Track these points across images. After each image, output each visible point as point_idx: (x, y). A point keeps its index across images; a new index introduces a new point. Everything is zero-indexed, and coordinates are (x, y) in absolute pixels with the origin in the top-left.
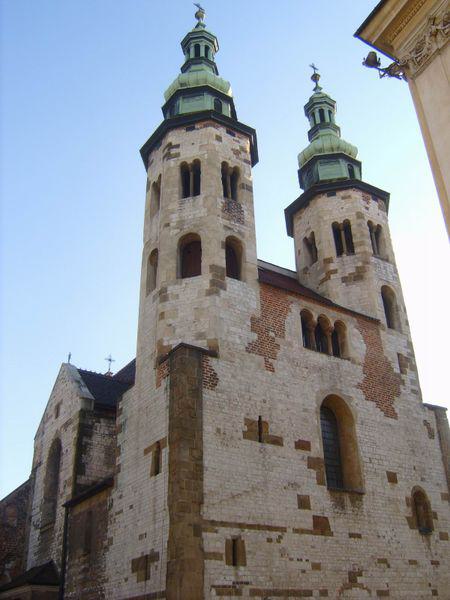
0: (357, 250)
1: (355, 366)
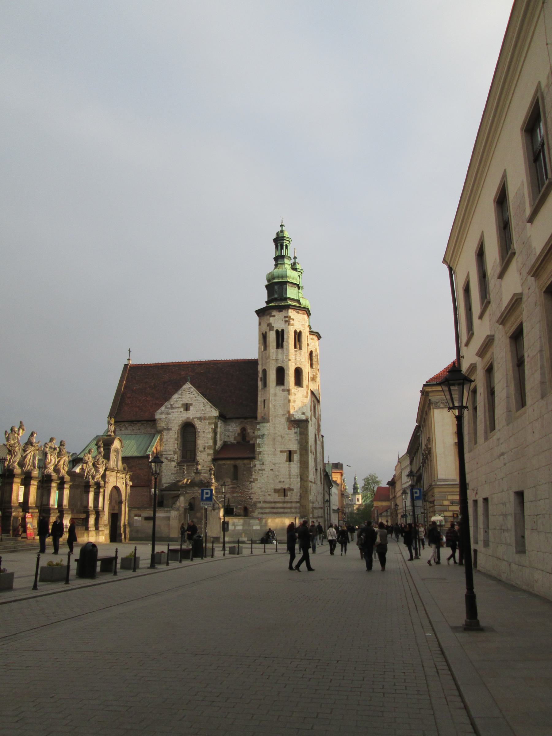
0: (314, 367)
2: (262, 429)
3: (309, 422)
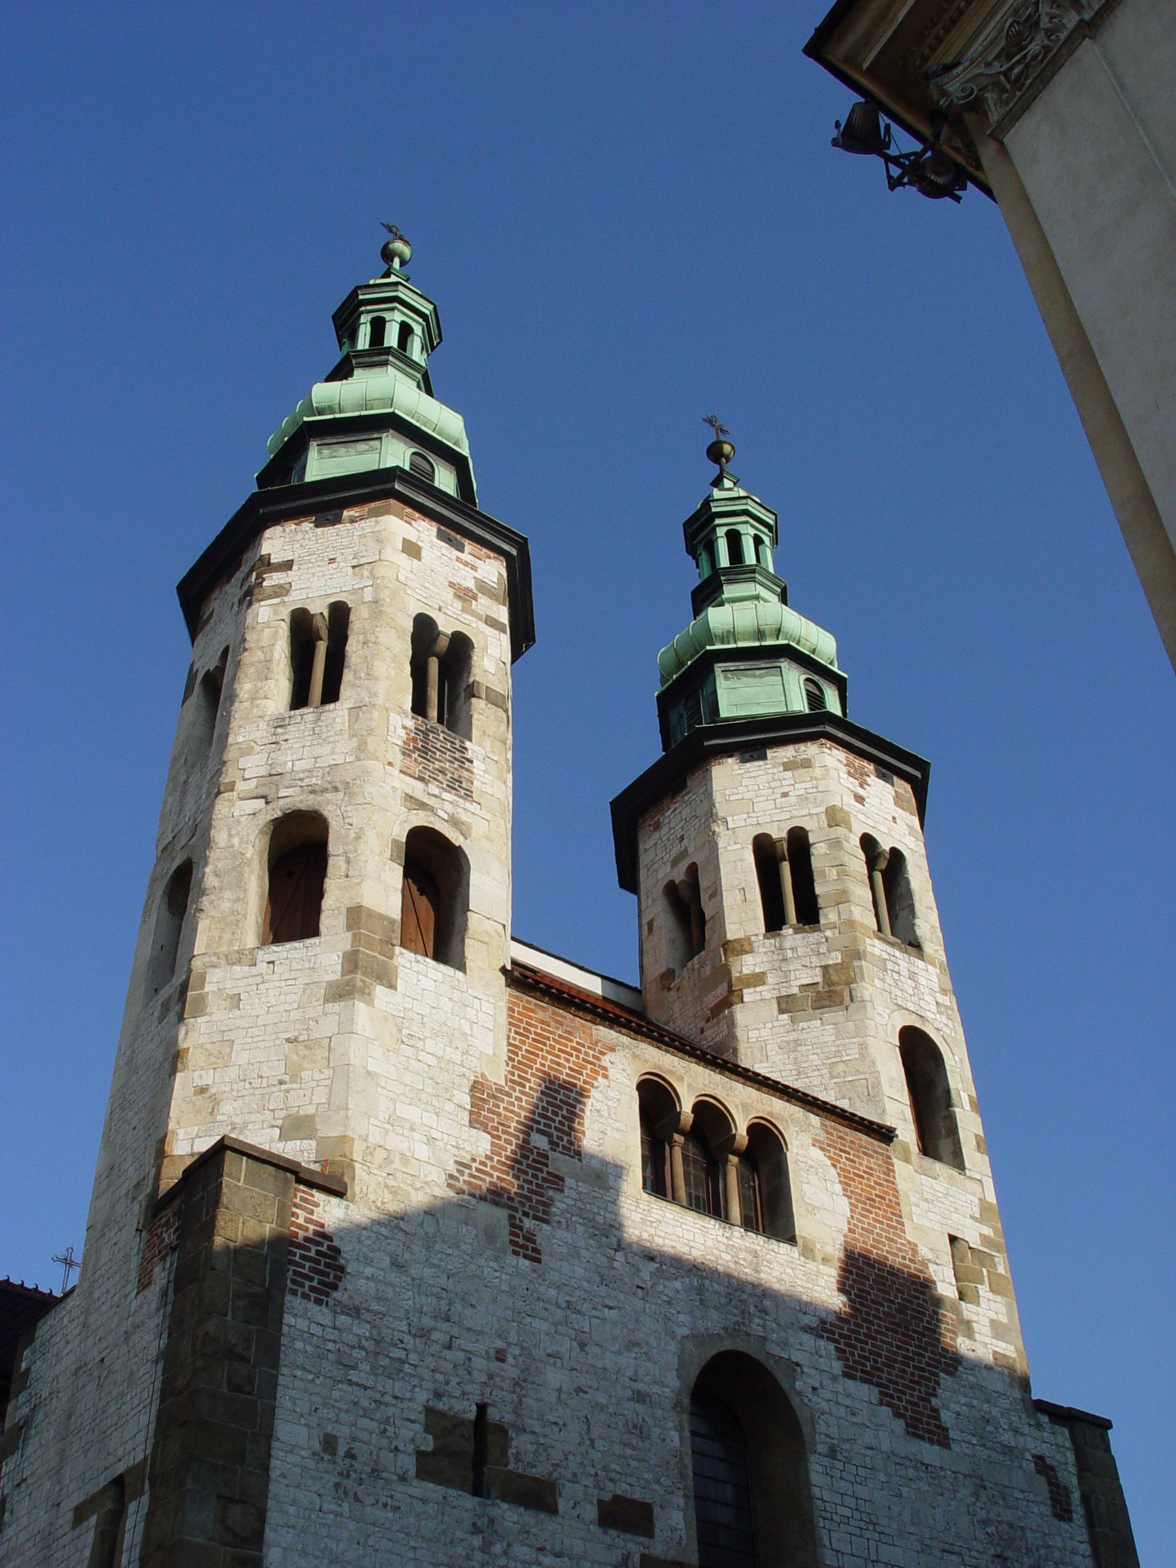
0: (828, 916)
1: (811, 1266)
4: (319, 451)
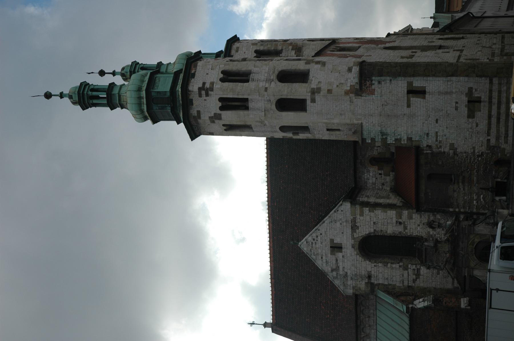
0: (280, 48)
2: (372, 135)
3: (364, 61)
4: (156, 89)
